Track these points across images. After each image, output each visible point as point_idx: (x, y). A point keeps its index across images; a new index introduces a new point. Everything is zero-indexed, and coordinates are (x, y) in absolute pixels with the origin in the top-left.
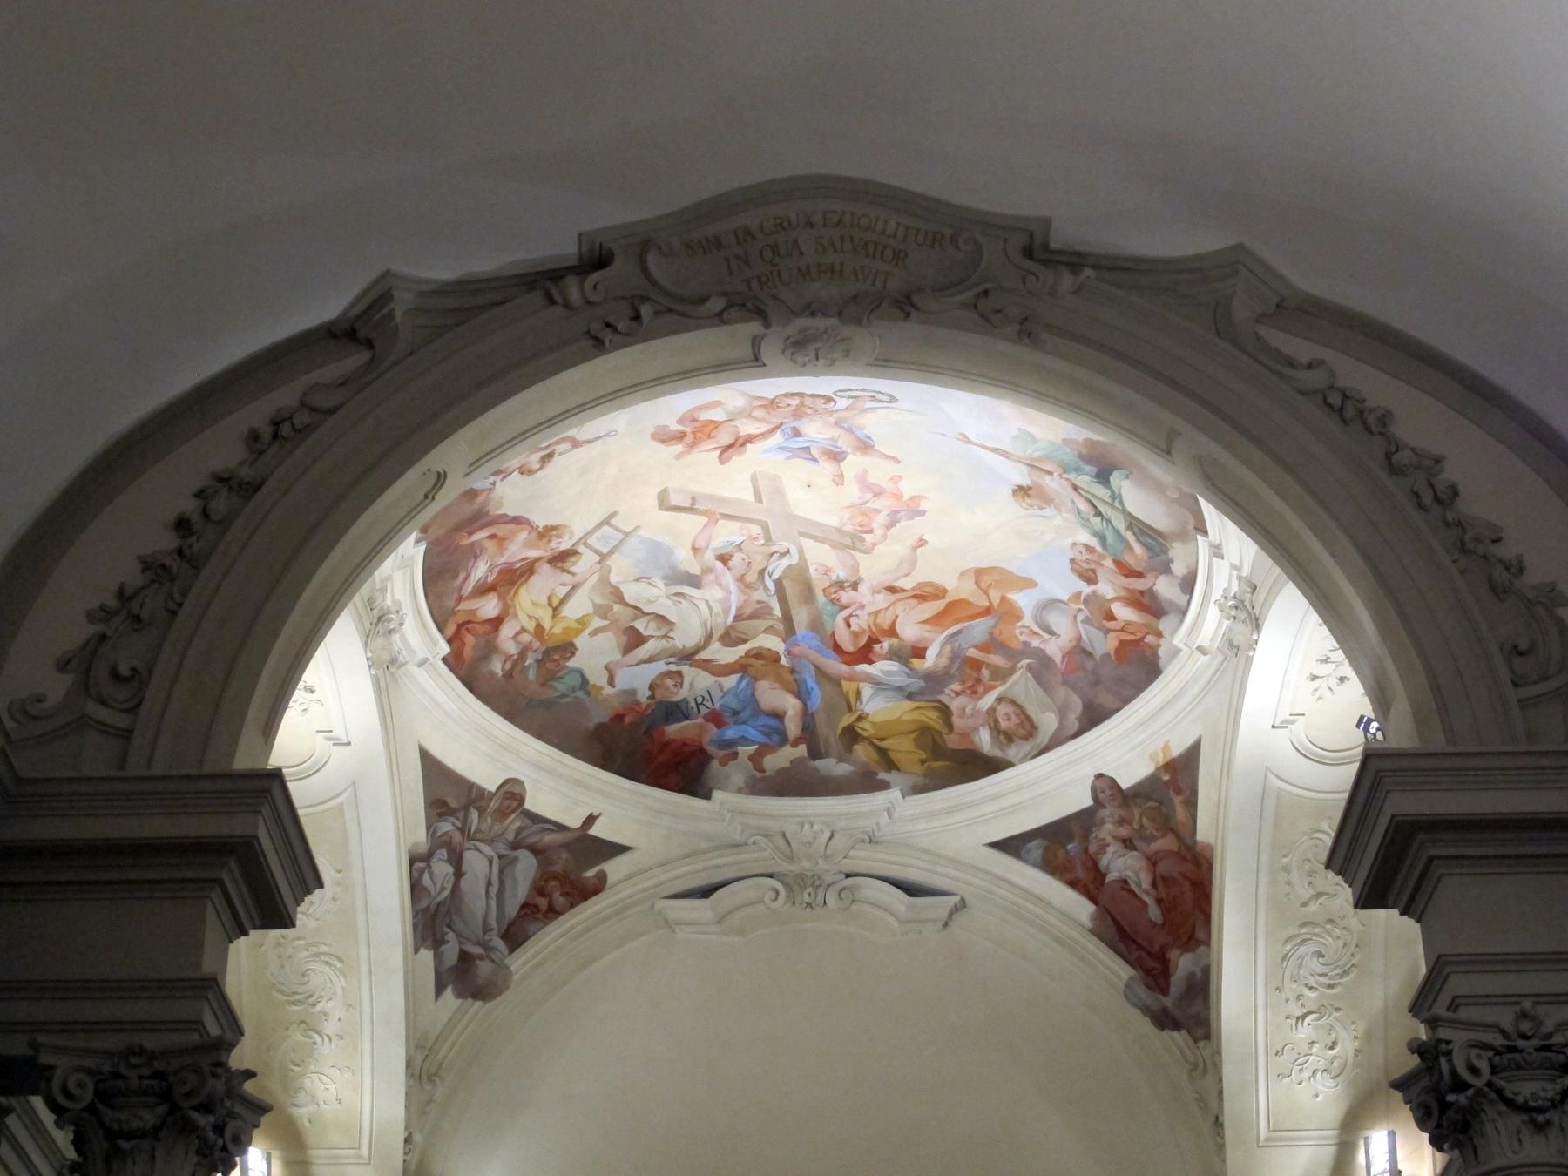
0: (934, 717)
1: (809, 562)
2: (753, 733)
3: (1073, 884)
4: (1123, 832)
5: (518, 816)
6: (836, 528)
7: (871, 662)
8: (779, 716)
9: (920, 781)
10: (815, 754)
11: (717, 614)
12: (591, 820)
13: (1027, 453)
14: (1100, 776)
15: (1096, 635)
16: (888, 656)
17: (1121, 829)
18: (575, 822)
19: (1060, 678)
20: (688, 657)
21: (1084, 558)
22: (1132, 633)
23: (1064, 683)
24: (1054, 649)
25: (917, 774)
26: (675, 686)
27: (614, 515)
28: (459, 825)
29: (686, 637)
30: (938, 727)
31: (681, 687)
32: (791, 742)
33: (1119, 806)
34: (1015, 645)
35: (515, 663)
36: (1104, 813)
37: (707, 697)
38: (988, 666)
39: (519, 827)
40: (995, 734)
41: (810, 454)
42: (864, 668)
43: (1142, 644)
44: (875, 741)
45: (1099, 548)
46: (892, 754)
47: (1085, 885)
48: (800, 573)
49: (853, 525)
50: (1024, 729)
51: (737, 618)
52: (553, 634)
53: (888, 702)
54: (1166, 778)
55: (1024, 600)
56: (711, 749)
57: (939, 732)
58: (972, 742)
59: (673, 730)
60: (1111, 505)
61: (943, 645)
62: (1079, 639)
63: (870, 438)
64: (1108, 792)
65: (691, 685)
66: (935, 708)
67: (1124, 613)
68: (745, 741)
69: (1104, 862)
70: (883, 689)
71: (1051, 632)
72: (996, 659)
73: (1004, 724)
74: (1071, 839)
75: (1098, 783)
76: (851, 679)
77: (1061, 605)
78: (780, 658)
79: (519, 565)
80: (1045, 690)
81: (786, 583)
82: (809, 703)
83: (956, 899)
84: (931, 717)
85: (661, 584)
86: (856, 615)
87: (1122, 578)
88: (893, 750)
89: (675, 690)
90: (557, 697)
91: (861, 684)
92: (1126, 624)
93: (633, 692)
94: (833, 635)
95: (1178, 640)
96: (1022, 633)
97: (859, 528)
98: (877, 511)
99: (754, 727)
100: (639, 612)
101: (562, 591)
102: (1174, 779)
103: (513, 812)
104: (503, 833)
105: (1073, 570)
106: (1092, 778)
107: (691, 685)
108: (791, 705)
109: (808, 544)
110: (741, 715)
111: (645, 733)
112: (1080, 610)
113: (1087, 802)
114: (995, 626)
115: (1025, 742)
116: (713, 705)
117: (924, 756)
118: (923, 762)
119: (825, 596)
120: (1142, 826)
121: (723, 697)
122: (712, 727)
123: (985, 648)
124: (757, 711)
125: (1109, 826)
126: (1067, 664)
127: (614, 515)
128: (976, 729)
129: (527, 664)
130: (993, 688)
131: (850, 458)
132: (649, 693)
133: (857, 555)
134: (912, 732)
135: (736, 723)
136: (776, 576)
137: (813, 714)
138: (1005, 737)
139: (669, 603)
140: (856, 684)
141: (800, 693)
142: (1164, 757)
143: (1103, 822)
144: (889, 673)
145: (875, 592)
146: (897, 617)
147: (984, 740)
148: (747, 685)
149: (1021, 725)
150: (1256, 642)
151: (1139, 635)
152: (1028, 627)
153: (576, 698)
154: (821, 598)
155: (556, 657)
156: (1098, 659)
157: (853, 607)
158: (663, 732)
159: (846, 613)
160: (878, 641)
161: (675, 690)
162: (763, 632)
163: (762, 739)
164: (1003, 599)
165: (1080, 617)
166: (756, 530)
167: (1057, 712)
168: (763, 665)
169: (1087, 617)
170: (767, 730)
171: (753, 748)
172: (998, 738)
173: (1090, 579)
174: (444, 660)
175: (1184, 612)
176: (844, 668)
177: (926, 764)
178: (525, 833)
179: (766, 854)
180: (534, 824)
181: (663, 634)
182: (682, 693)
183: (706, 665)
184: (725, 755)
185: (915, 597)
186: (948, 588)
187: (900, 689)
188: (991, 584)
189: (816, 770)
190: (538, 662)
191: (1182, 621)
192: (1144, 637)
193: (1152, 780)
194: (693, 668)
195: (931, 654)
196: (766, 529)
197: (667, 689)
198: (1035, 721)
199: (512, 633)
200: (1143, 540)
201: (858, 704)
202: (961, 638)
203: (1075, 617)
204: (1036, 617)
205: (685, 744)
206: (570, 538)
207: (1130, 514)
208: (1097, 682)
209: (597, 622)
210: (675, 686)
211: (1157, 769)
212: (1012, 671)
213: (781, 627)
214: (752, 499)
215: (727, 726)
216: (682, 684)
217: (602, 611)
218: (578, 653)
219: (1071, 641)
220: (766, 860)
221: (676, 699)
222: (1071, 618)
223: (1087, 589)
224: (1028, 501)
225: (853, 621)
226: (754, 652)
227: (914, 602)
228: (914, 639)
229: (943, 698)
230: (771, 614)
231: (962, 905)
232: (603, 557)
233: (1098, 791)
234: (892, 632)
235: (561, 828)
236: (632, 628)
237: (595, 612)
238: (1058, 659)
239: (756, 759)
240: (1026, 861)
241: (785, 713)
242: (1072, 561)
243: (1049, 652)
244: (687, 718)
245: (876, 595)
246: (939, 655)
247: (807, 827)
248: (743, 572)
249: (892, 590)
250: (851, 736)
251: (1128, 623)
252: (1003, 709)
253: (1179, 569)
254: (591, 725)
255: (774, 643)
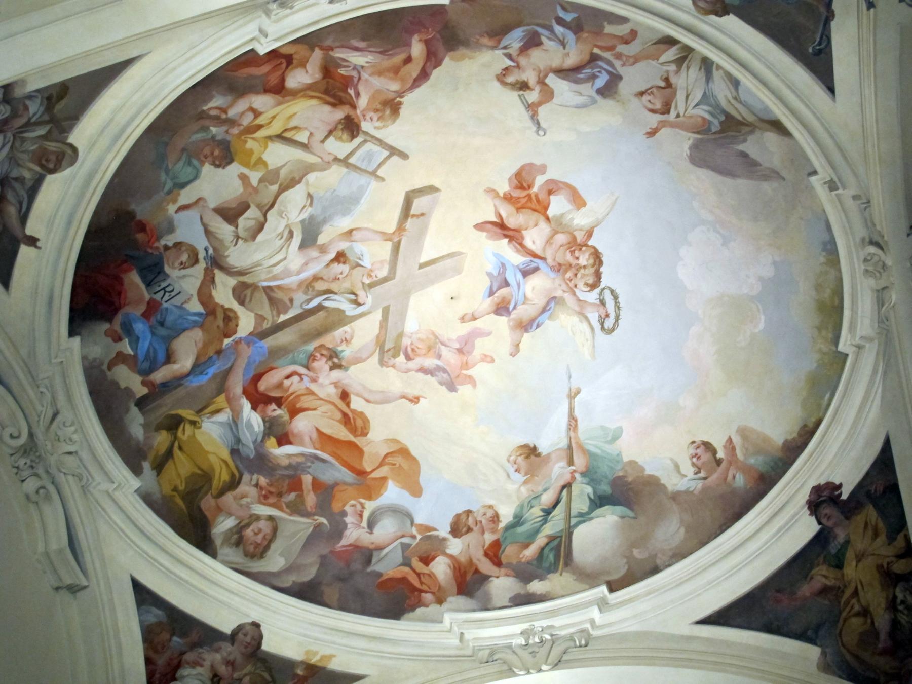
0: (222, 479)
1: (352, 324)
2: (144, 345)
3: (148, 661)
4: (223, 670)
5: (37, 172)
6: (403, 332)
7: (254, 408)
8: (169, 358)
9: (157, 496)
10: (141, 403)
11: (269, 272)
12: (32, 241)
13: (586, 441)
14: (256, 625)
15: (398, 557)
16: (267, 419)
17: (224, 667)
18: (31, 228)
19: (325, 551)
20: (216, 263)
21: (479, 519)
22: (422, 583)
23: (323, 558)
24: (354, 534)
25: (161, 491)
26: (182, 263)
27: (404, 156)
28: (33, 120)
29: (237, 257)
30: (215, 483)
31: (180, 269)
32: (147, 379)
33: (243, 654)
34: (336, 506)
35: (217, 118)
36: (227, 647)
37: (173, 294)
38: (301, 497)
39: (24, 178)
40: (234, 531)
41: (499, 288)
42: (246, 405)
43: (416, 593)
44: (176, 444)
45: (502, 525)
46: (170, 462)
47: (156, 670)
48: (339, 319)
49: (412, 344)
50: (255, 548)
51: (268, 290)
52: (246, 142)
53: (221, 437)
54: (300, 672)
55: (393, 494)
56: (119, 318)
57: (210, 488)
58: (215, 517)
59: (134, 278)
60: (569, 516)
61: (302, 455)
62: (380, 548)
63: (538, 326)
64: (248, 639)
65: (184, 276)
66: (233, 475)
67: (441, 568)
68: (135, 342)
69: (185, 671)
70: (231, 429)
71: (371, 525)
72: (311, 499)
73: (249, 532)
74: (184, 635)
75: (248, 628)
76: (228, 400)
77: (409, 523)
78: (229, 337)
79: (351, 92)
80: (304, 546)
81: (322, 314)
82: (190, 378)
83: (85, 583)
84: (222, 476)
85: (305, 215)
86: (302, 379)
87: (481, 553)
88: (174, 462)
89: (177, 265)
90: (167, 166)
91: (228, 410)
92: (429, 575)
93: (171, 229)
94: (272, 369)
95: (448, 618)
96: (353, 506)
97: (409, 350)
98: (439, 357)
99: (151, 343)
100: (266, 210)
101: (302, 137)
102: (305, 678)
103: (42, 166)
104: (19, 165)
105: (458, 516)
106: (250, 620)
107: (184, 276)
108: (184, 363)
109: (378, 315)
110: (159, 328)
111: (126, 255)
112: (414, 537)
113: (227, 629)
114: (345, 484)
115: (243, 557)
116: (166, 302)
117: (182, 488)
118: (175, 489)
119: (315, 349)
120: (240, 680)
121: (176, 306)
122: (143, 308)
123: (317, 485)
124: (168, 340)
125: (218, 657)
126: (346, 551)
127: (404, 156)
128: (230, 514)
129: (212, 128)
130: (280, 508)
131: (503, 320)
132: (170, 244)
133: (376, 357)
134: (199, 468)
135: (151, 328)
136: (327, 304)
137: (181, 385)
138: (237, 538)
139: (281, 228)
140: (225, 404)
141: (198, 367)
142: (320, 661)
143: (218, 650)
144: (249, 425)
145: (336, 384)
146: (315, 409)
147: (223, 526)
148: (195, 322)
149: (257, 545)
150: (540, 671)
151: (424, 588)
152: (363, 508)
153: (165, 184)
154: (311, 347)
155: (217, 152)
156: (369, 570)
157: (311, 374)
158: (130, 270)
159: (302, 370)
160: (279, 405)
161: (177, 265)
162: (256, 314)
163: (141, 357)
164: (384, 479)
165: (406, 540)
166: (383, 273)
167: (287, 566)
168: (218, 327)
169: (409, 545)
170: (152, 354)
171: (129, 351)
172: (233, 534)
173: (457, 529)
174: (252, 50)
175: (487, 609)
176: (238, 390)
177: (175, 493)
178: (17, 186)
179: (39, 408)
180: (27, 193)
181: (241, 235)
182: (173, 272)
183: (209, 280)
184: (116, 332)
185: (345, 415)
186: (369, 436)
187: (238, 441)
188: (395, 464)
189: (127, 410)
190: (213, 138)
191: (474, 611)
192: (426, 592)
193: (288, 665)
194: (203, 272)
195: (288, 449)
196: (385, 280)
197: (178, 257)
198: (269, 553)
199: (255, 106)
200: (547, 550)
201: (208, 415)
202: (317, 463)
203: (403, 536)
204: (379, 509)
205: (119, 294)
206: (375, 128)
207: (570, 535)
208: (342, 579)
209: (255, 177)
210: (182, 263)
211: (302, 662)
212: (307, 515)
213: (266, 325)
214: (423, 259)
215: (146, 321)
216: (184, 268)
217: (271, 177)
218: (220, 170)
219: (373, 543)
220: (35, 409)
221: (167, 269)
222: (400, 533)
223: (444, 531)
224: (520, 459)
225: (296, 379)
226: (231, 315)
227: (339, 416)
228: (296, 431)
229: (246, 477)
230: (279, 314)
231: (74, 589)
232: (344, 162)
233: (244, 631)
234: (294, 412)
235: (23, 219)
236: (247, 207)
237: (269, 172)
238: (344, 542)
239: (120, 358)
240: (140, 615)
241: (174, 363)
242: (468, 512)
243: (347, 533)
244: (148, 285)
245: (332, 386)
246: (289, 456)
247: (73, 428)
248: (324, 277)
249: (345, 396)
250: (174, 424)
251: (431, 575)
252: (263, 525)
253: (536, 587)
254: (133, 207)
255: (246, 324)
